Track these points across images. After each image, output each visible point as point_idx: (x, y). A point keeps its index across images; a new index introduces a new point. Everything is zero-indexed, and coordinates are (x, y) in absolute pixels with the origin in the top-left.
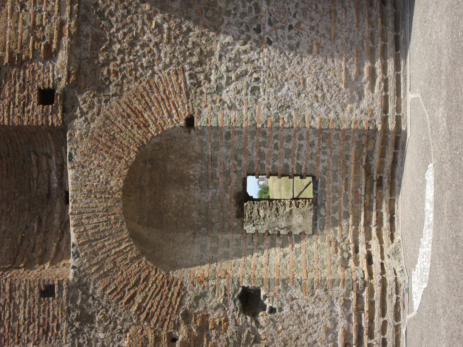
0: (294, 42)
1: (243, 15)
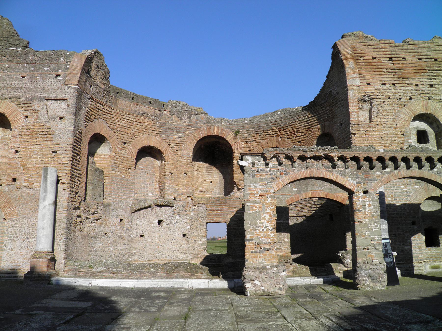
0: (23, 248)
1: (32, 234)
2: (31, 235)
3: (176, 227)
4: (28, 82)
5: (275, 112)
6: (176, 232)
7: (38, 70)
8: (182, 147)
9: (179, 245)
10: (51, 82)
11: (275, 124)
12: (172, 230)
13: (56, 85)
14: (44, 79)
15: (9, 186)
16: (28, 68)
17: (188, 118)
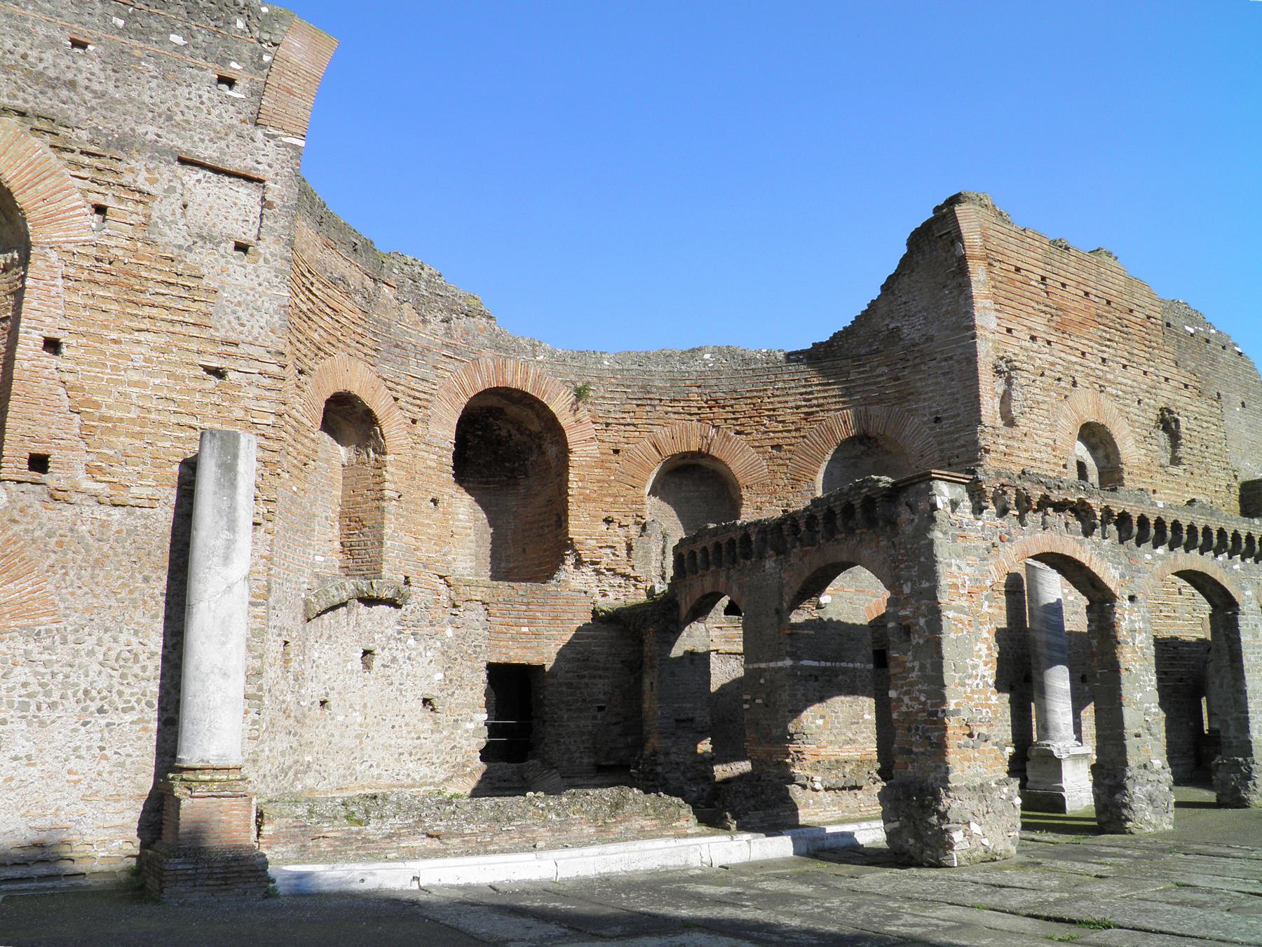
0: (83, 752)
1: (120, 693)
2: (115, 697)
3: (408, 675)
4: (103, 70)
5: (693, 350)
6: (406, 690)
7: (143, 34)
8: (429, 412)
9: (413, 735)
10: (200, 97)
11: (699, 387)
12: (397, 683)
13: (220, 116)
14: (170, 77)
15: (11, 485)
16: (98, 11)
17: (443, 321)
